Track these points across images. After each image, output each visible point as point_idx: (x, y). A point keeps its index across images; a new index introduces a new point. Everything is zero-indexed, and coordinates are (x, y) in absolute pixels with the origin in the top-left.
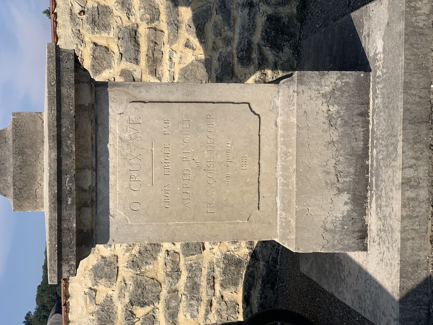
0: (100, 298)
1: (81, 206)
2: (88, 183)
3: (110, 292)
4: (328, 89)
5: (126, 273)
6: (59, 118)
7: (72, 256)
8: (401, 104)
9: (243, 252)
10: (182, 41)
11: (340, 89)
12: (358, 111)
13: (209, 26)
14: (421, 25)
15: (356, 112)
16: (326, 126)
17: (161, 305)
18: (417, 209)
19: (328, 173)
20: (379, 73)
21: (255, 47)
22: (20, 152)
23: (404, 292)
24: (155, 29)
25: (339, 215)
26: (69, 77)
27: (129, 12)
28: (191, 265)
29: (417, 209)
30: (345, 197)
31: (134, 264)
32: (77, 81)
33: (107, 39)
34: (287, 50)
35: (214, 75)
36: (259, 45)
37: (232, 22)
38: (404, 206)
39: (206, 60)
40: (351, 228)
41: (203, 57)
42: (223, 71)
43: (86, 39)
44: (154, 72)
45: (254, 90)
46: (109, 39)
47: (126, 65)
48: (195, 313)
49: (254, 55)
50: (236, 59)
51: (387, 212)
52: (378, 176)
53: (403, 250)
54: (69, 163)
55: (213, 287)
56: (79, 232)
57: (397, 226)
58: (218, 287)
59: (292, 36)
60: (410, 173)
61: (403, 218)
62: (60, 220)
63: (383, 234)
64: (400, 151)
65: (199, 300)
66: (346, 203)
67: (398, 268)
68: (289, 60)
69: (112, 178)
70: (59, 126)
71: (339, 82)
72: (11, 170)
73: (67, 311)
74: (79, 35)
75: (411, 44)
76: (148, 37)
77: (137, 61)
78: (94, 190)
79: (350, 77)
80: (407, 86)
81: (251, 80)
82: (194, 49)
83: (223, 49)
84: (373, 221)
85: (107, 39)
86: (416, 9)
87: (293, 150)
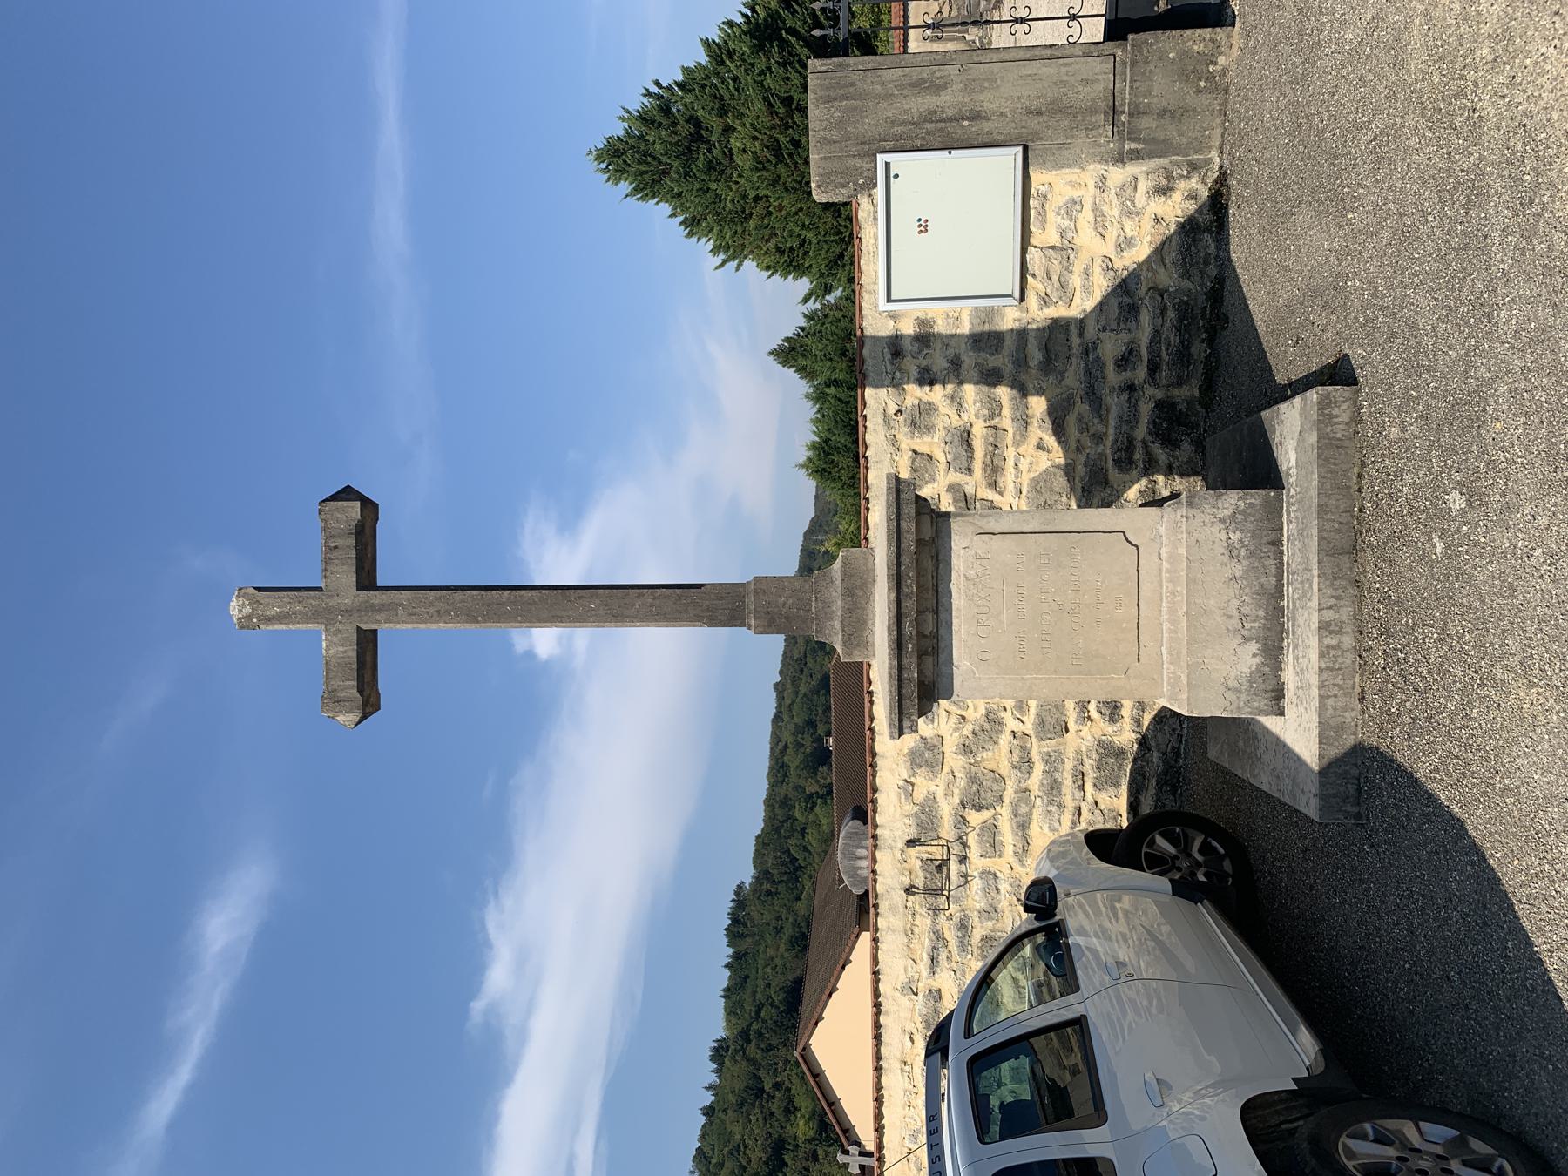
0: (919, 796)
1: (922, 654)
2: (929, 628)
3: (933, 788)
4: (1227, 512)
5: (955, 761)
6: (898, 556)
7: (914, 710)
8: (1315, 531)
9: (1126, 736)
10: (1033, 441)
11: (1243, 512)
12: (1269, 539)
13: (1071, 420)
14: (1339, 436)
15: (1265, 540)
16: (1226, 558)
17: (1005, 811)
18: (1340, 660)
19: (1230, 617)
20: (1293, 492)
21: (1139, 445)
22: (849, 593)
23: (1325, 761)
24: (995, 428)
25: (1247, 670)
26: (909, 510)
27: (960, 408)
28: (1048, 754)
29: (1340, 660)
30: (1254, 647)
31: (966, 749)
32: (918, 513)
33: (930, 444)
34: (1187, 448)
35: (1079, 485)
36: (1144, 442)
37: (1104, 412)
38: (1322, 655)
39: (1067, 465)
40: (1262, 687)
41: (1062, 461)
42: (1094, 487)
43: (903, 446)
44: (993, 485)
45: (1127, 513)
46: (934, 444)
47: (955, 477)
48: (1056, 825)
49: (1138, 456)
50: (1110, 462)
51: (1302, 667)
52: (1294, 620)
53: (1322, 709)
54: (910, 605)
55: (1082, 787)
56: (921, 683)
57: (1314, 680)
58: (1089, 787)
59: (1194, 427)
60: (1329, 615)
61: (1321, 670)
62: (900, 668)
63: (1300, 693)
64: (1315, 588)
65: (1061, 806)
66: (1255, 655)
67: (1316, 732)
68: (1190, 460)
69: (955, 622)
70: (899, 564)
71: (1241, 503)
72: (840, 613)
73: (875, 811)
74: (893, 441)
75: (1326, 460)
76: (986, 438)
77: (970, 471)
78: (936, 636)
79: (1256, 497)
80: (1322, 510)
81: (1132, 493)
82: (1049, 452)
83: (1091, 449)
84: (1289, 677)
85: (930, 444)
86: (1331, 416)
87: (1182, 588)
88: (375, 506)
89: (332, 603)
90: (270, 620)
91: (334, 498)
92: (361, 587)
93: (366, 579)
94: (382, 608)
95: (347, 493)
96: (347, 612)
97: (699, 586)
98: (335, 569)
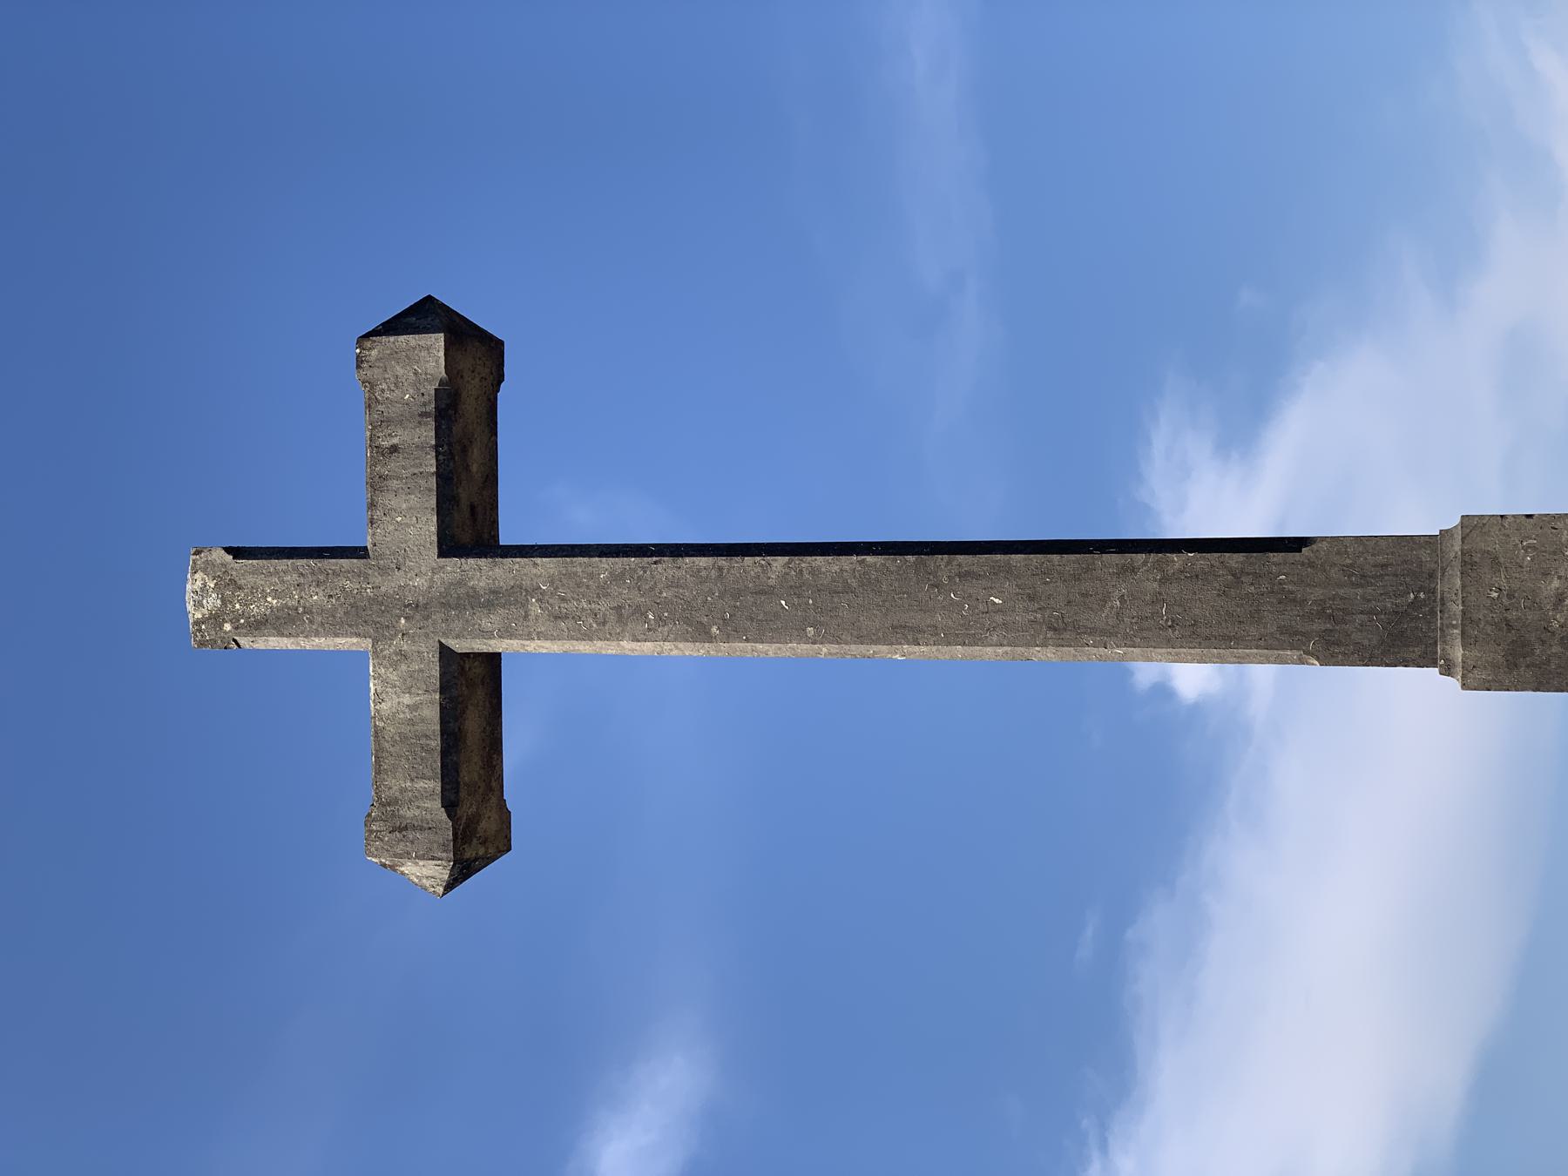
88: (494, 347)
89: (388, 586)
90: (258, 626)
91: (392, 327)
92: (449, 546)
93: (468, 526)
94: (493, 600)
95: (425, 315)
96: (418, 608)
97: (1296, 544)
98: (394, 502)
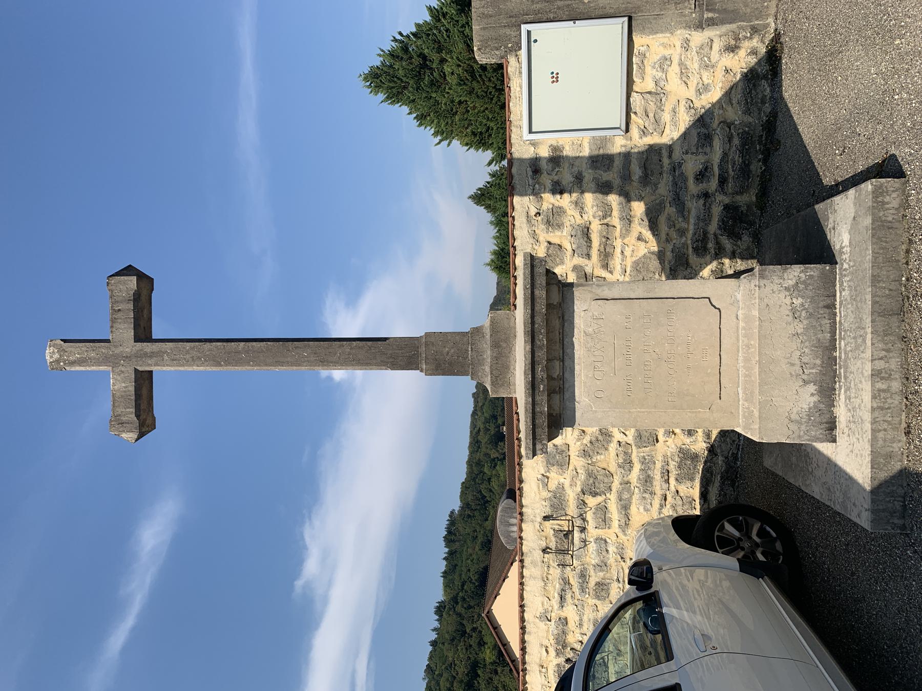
0: (552, 485)
1: (551, 393)
2: (556, 373)
3: (562, 480)
4: (791, 283)
5: (577, 462)
6: (533, 317)
7: (545, 436)
8: (869, 297)
9: (700, 446)
10: (635, 234)
11: (804, 282)
12: (825, 303)
13: (662, 219)
14: (890, 219)
15: (822, 304)
16: (790, 319)
17: (613, 497)
18: (889, 401)
19: (793, 365)
20: (846, 266)
21: (711, 237)
22: (496, 345)
23: (876, 483)
24: (607, 225)
25: (806, 407)
26: (541, 280)
27: (582, 211)
28: (644, 457)
29: (889, 401)
30: (812, 388)
31: (585, 453)
32: (548, 284)
33: (561, 237)
34: (746, 239)
35: (667, 266)
36: (715, 235)
37: (686, 213)
38: (874, 397)
39: (659, 252)
40: (818, 420)
41: (656, 249)
42: (678, 265)
43: (541, 239)
44: (606, 266)
46: (563, 237)
47: (578, 261)
48: (649, 506)
49: (710, 245)
50: (690, 250)
51: (856, 404)
52: (846, 368)
53: (874, 440)
54: (541, 354)
55: (667, 481)
56: (550, 415)
57: (867, 417)
58: (672, 481)
59: (751, 224)
60: (880, 365)
61: (873, 409)
62: (534, 404)
63: (852, 426)
64: (869, 343)
65: (653, 493)
66: (812, 395)
67: (868, 459)
68: (748, 248)
69: (577, 367)
70: (533, 323)
71: (802, 275)
72: (489, 360)
73: (521, 496)
74: (534, 235)
75: (879, 238)
76: (600, 232)
77: (588, 256)
78: (562, 378)
79: (814, 270)
80: (875, 279)
81: (706, 272)
82: (646, 242)
83: (677, 240)
84: (841, 412)
85: (561, 237)
86: (883, 203)
87: (755, 342)
89: (117, 351)
90: (72, 363)
91: (118, 274)
92: (137, 339)
93: (143, 333)
94: (152, 355)
95: (129, 270)
96: (127, 358)
97: (385, 339)
